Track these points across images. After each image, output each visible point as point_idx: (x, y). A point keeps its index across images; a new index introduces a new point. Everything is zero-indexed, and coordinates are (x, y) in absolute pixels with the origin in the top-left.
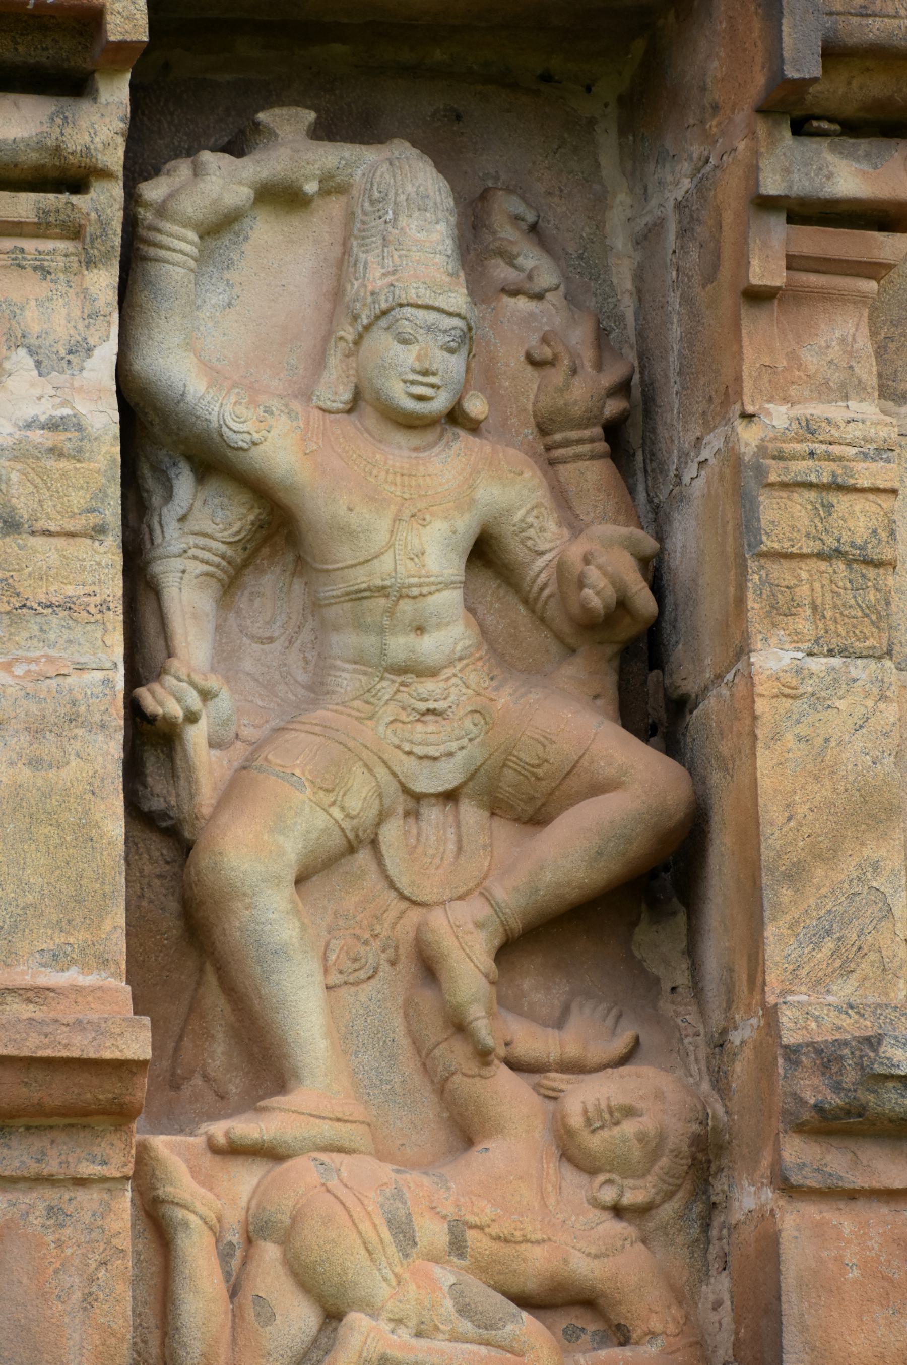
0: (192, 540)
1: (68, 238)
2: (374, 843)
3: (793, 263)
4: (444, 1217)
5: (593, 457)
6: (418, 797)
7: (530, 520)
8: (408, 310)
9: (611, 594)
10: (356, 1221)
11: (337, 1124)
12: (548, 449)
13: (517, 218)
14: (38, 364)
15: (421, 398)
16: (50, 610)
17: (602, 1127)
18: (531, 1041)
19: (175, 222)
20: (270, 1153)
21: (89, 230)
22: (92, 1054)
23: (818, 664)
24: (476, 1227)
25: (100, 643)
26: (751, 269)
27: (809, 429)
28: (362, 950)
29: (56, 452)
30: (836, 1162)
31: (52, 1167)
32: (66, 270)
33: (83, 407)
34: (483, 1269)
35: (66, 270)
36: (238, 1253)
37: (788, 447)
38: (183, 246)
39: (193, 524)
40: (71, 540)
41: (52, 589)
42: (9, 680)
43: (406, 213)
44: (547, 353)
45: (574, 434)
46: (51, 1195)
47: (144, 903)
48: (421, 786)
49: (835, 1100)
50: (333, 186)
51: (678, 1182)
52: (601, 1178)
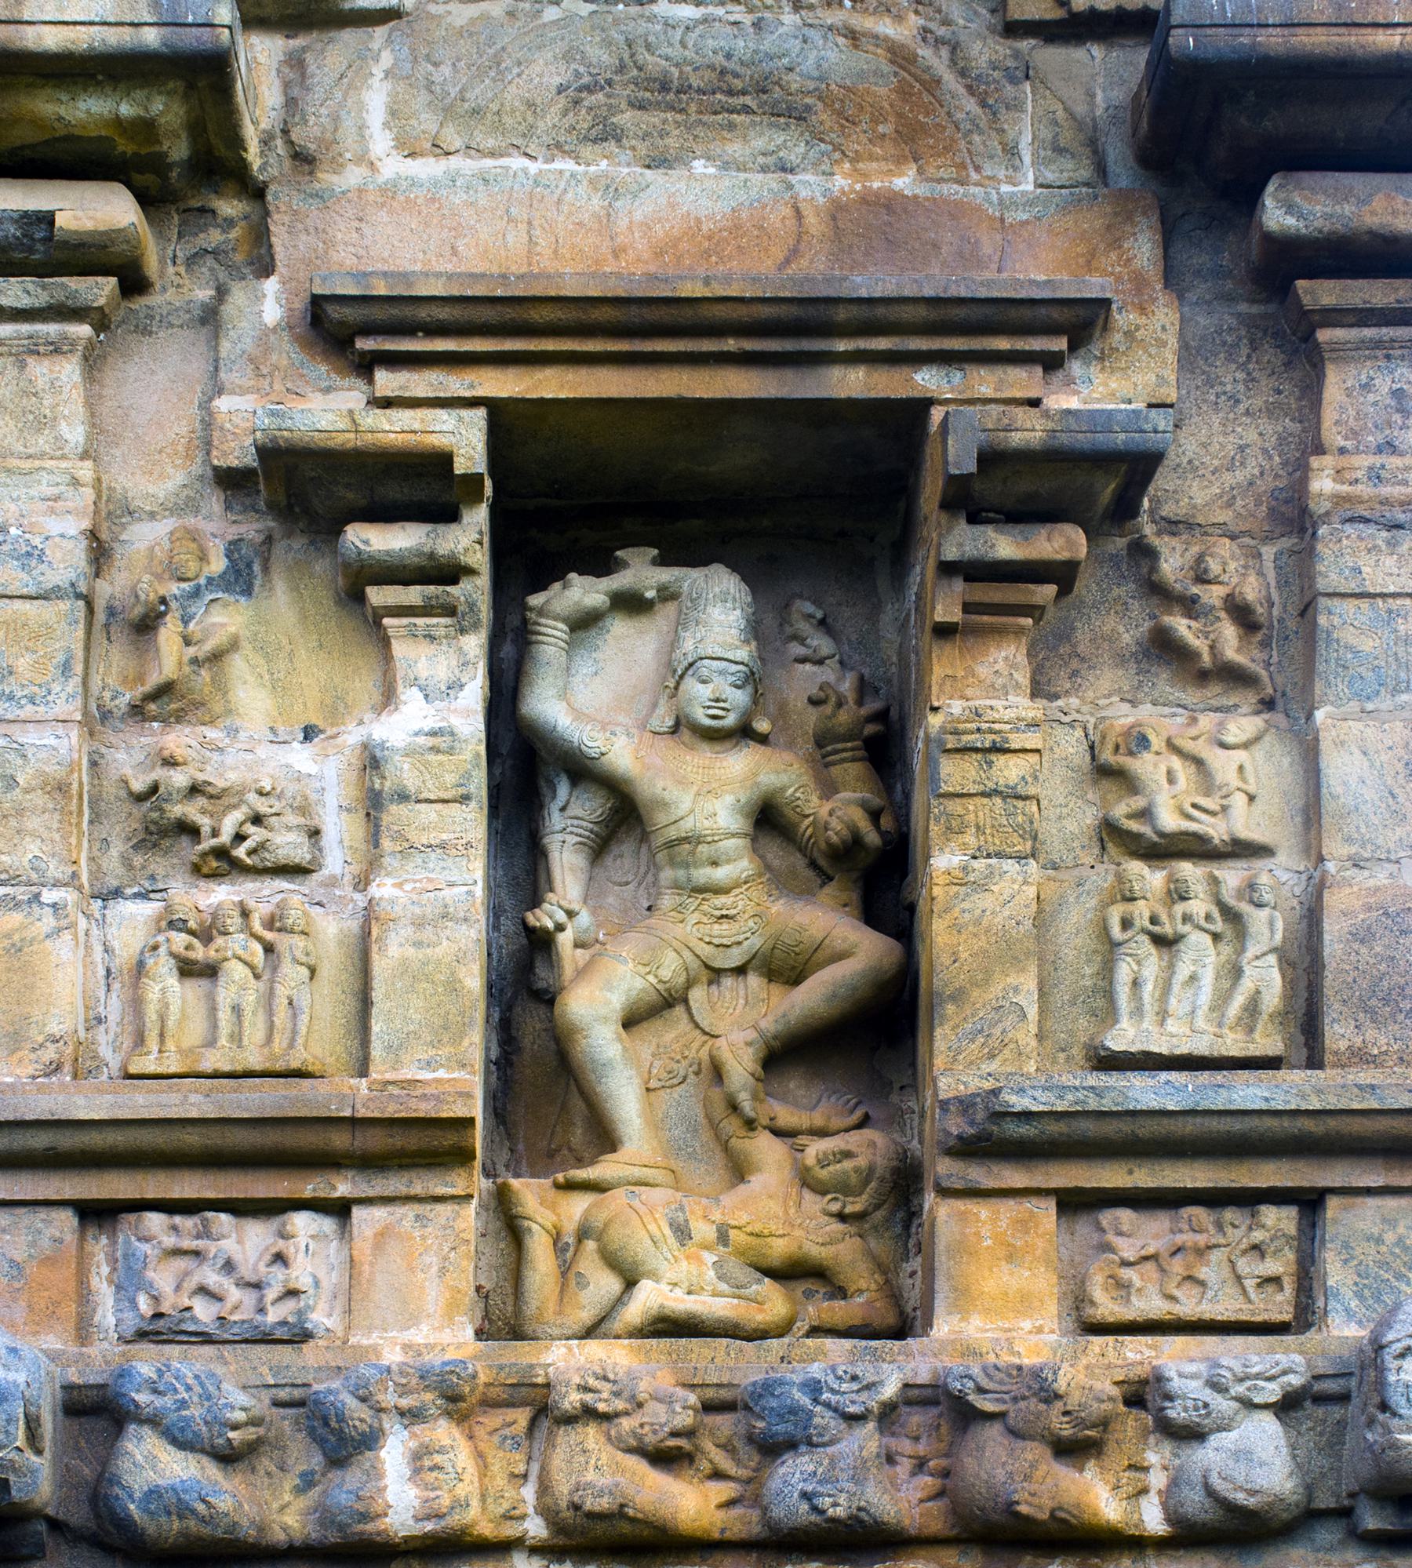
5: (853, 760)
12: (824, 757)
14: (426, 696)
19: (548, 617)
21: (460, 609)
32: (446, 637)
38: (555, 632)
42: (401, 894)
45: (839, 746)
50: (667, 595)
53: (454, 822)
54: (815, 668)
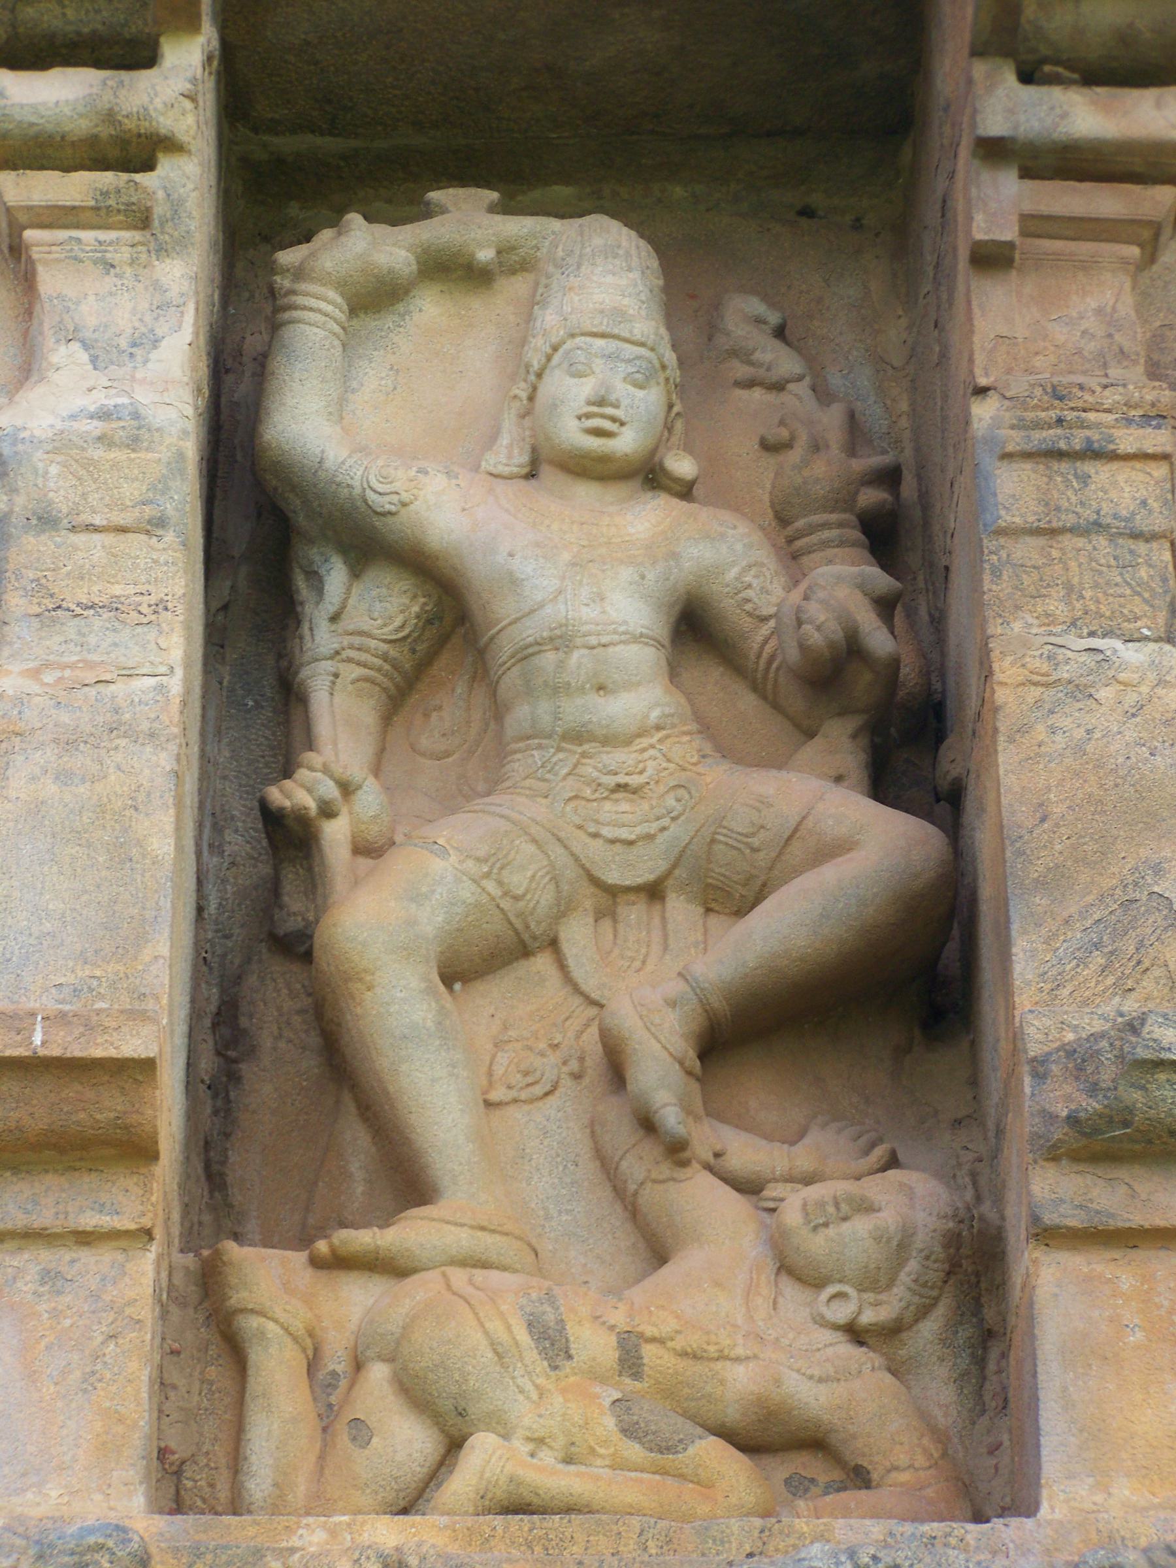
0: (347, 640)
1: (136, 228)
2: (554, 944)
4: (612, 1328)
5: (841, 544)
6: (613, 892)
8: (580, 340)
9: (835, 631)
10: (482, 1319)
11: (479, 1234)
12: (790, 541)
13: (759, 321)
14: (94, 360)
15: (599, 433)
16: (92, 612)
17: (826, 1225)
18: (746, 1152)
19: (312, 280)
20: (393, 1268)
21: (158, 211)
24: (653, 1340)
25: (153, 646)
26: (975, 225)
28: (538, 1062)
31: (45, 1218)
32: (133, 262)
33: (143, 397)
35: (133, 262)
36: (343, 1383)
38: (323, 305)
39: (347, 623)
40: (122, 537)
41: (95, 589)
42: (36, 688)
43: (600, 281)
44: (785, 433)
46: (46, 1256)
47: (282, 1044)
48: (613, 876)
49: (1094, 1105)
51: (935, 1293)
52: (831, 1290)
53: (135, 566)
54: (771, 397)
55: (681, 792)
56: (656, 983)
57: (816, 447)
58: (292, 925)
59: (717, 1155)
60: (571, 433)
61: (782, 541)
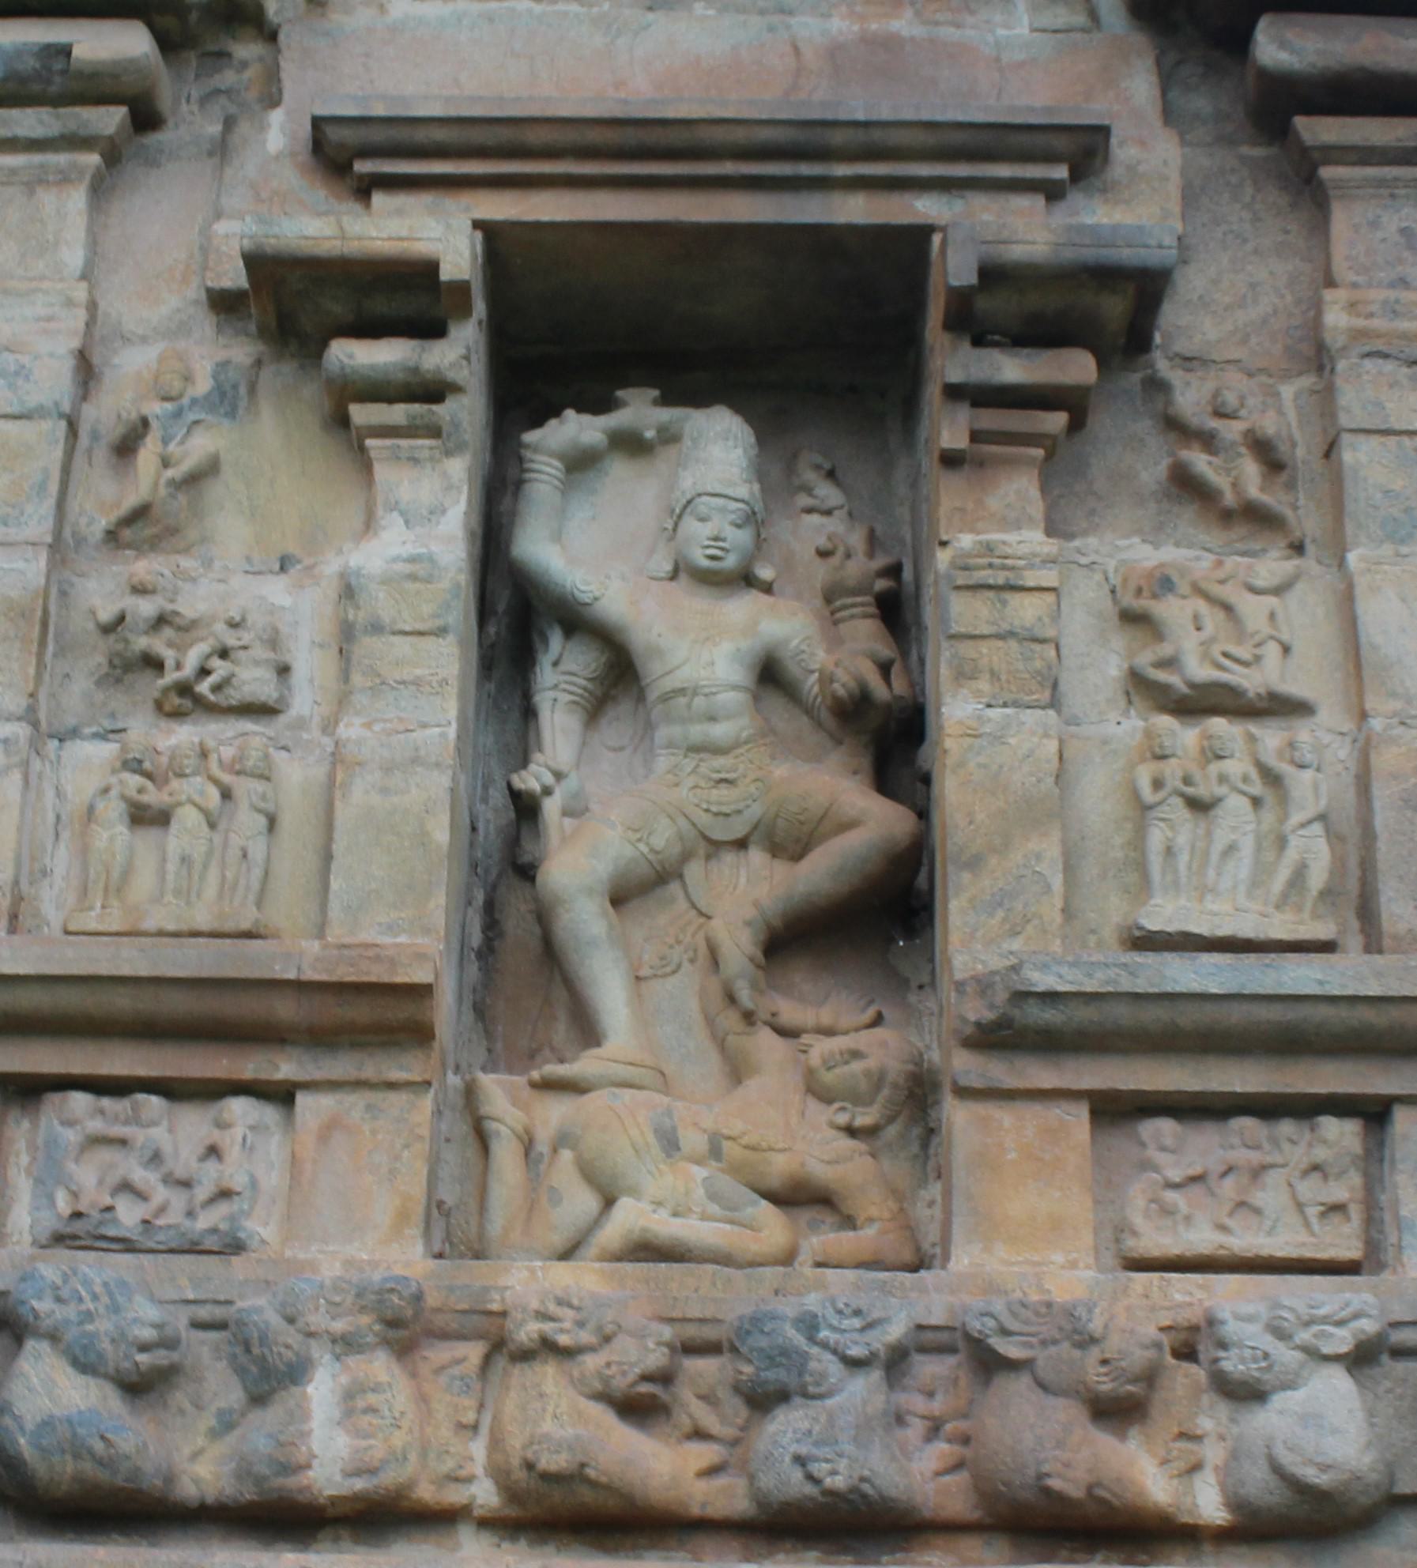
2: (681, 876)
3: (976, 436)
4: (705, 1131)
5: (865, 616)
7: (803, 647)
8: (705, 499)
9: (852, 684)
12: (832, 613)
14: (407, 522)
15: (713, 558)
18: (790, 1012)
21: (445, 429)
22: (386, 979)
23: (995, 713)
24: (729, 1138)
27: (989, 548)
29: (413, 577)
30: (1000, 1071)
32: (432, 459)
33: (435, 548)
34: (736, 1170)
37: (972, 561)
38: (548, 469)
39: (562, 667)
40: (422, 638)
42: (369, 734)
43: (718, 448)
44: (829, 546)
45: (850, 601)
48: (718, 835)
49: (989, 1016)
52: (836, 1105)
54: (824, 520)
55: (759, 784)
56: (745, 894)
57: (848, 556)
58: (526, 858)
59: (774, 1015)
60: (699, 558)
61: (828, 614)
